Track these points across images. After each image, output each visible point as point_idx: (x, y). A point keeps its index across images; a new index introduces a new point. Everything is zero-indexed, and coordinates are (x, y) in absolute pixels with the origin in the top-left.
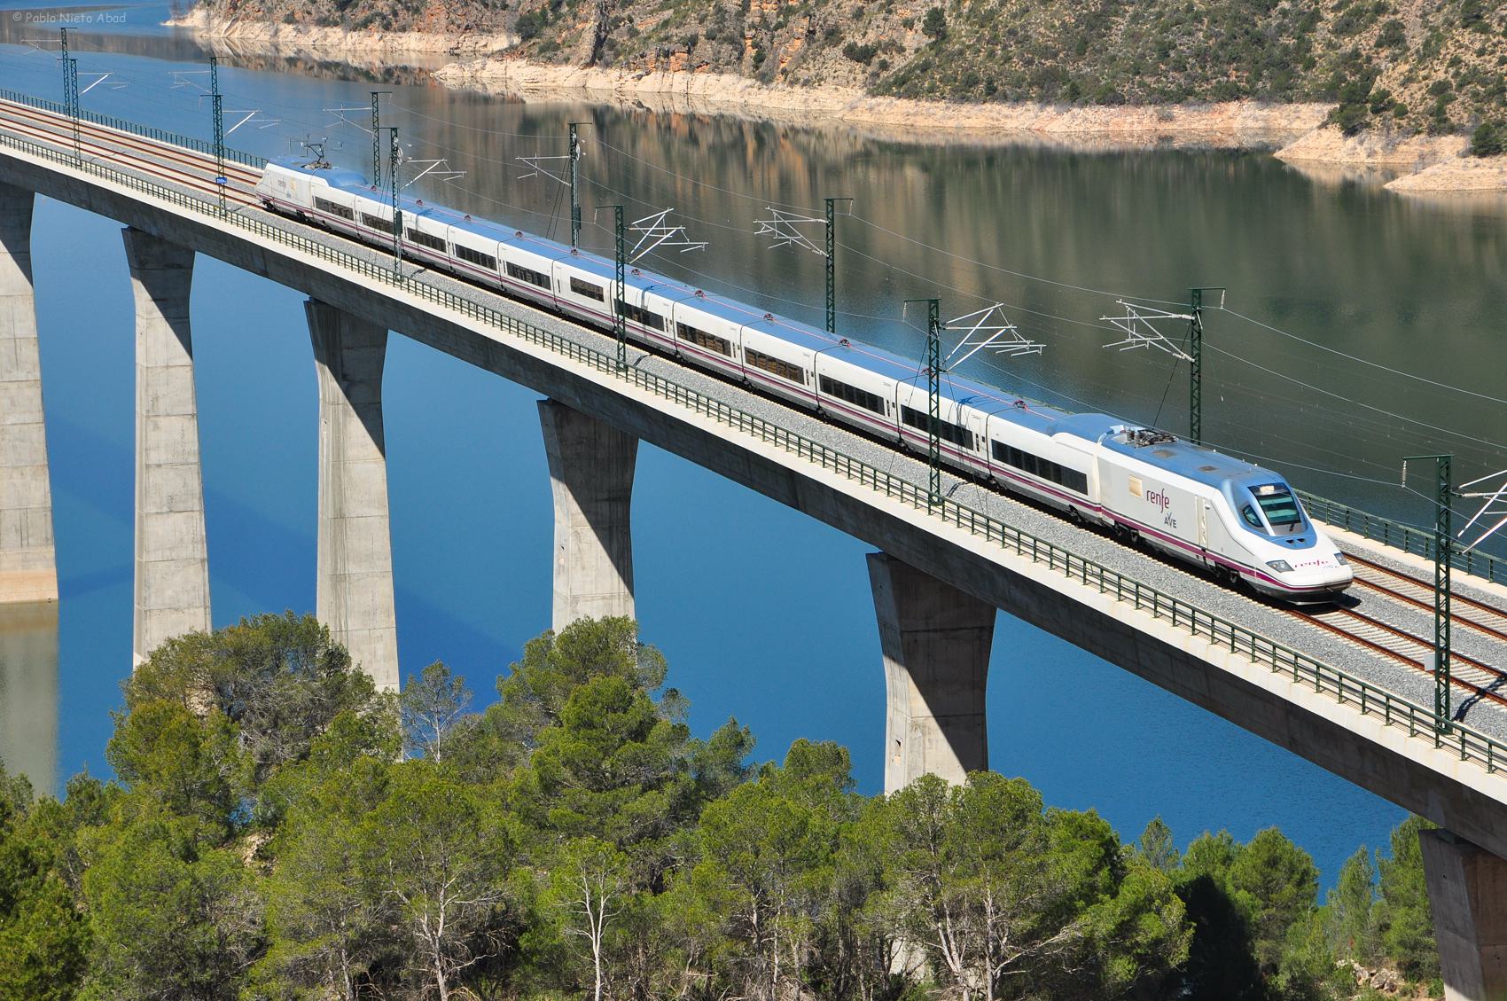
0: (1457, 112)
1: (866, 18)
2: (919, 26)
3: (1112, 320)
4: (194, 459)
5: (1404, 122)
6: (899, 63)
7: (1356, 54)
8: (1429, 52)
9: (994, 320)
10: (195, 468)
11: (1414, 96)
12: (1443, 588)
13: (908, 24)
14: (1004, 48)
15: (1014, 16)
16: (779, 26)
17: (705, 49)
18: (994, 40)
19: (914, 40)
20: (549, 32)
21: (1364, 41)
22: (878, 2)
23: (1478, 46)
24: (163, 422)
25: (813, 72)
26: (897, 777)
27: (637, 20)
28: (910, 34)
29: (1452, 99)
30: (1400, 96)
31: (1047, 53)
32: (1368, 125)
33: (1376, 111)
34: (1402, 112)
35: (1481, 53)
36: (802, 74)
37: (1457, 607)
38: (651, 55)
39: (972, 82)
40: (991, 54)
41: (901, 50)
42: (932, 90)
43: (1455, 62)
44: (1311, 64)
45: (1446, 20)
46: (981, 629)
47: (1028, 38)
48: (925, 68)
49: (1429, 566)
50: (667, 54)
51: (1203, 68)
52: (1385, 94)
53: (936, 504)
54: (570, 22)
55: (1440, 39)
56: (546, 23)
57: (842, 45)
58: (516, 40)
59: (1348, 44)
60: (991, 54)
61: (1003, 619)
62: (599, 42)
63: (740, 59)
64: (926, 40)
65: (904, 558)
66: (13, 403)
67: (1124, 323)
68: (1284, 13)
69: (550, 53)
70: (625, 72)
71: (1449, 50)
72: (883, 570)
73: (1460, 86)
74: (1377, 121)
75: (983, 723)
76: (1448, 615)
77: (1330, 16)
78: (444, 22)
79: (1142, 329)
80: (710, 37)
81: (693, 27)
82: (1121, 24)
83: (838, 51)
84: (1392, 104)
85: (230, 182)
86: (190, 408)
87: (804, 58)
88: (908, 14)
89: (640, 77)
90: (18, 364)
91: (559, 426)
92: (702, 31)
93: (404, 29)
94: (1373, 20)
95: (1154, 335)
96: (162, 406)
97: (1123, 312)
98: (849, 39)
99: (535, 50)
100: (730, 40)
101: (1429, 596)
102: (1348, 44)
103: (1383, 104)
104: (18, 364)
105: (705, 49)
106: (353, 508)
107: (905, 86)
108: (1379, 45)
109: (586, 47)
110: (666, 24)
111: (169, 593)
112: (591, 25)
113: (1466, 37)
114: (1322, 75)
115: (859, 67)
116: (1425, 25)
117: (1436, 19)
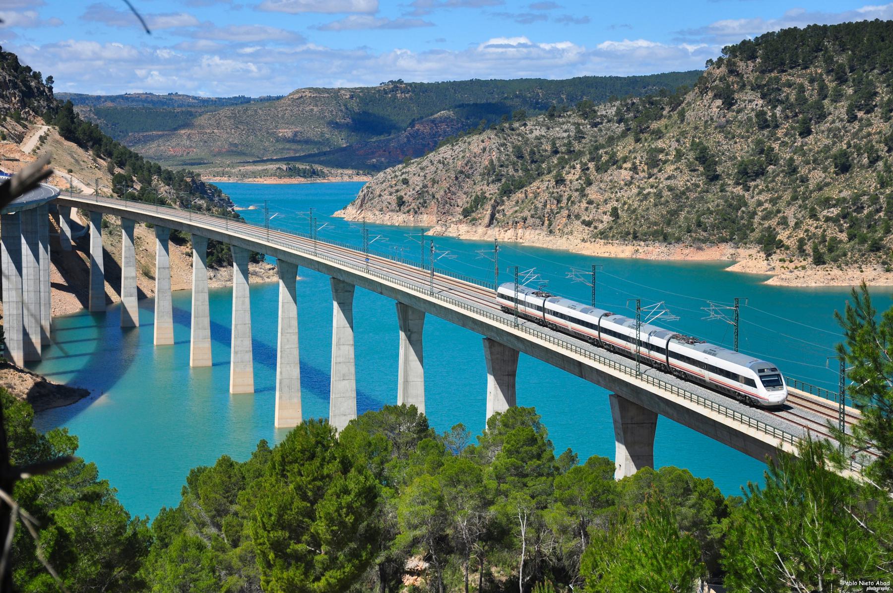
0: (808, 248)
1: (589, 211)
2: (609, 214)
3: (705, 309)
4: (352, 361)
5: (788, 252)
6: (601, 226)
7: (770, 227)
8: (797, 225)
9: (661, 308)
10: (353, 364)
11: (792, 243)
12: (843, 412)
13: (605, 213)
14: (640, 222)
15: (644, 211)
16: (557, 213)
17: (530, 221)
18: (637, 219)
19: (607, 218)
20: (474, 215)
21: (773, 222)
22: (224, 589)
23: (815, 225)
24: (342, 347)
25: (569, 229)
26: (619, 475)
27: (506, 211)
28: (605, 217)
29: (806, 244)
30: (787, 242)
31: (656, 224)
32: (775, 253)
33: (777, 248)
34: (788, 248)
35: (816, 228)
36: (566, 230)
37: (847, 419)
38: (510, 223)
39: (628, 233)
40: (635, 224)
41: (602, 222)
42: (613, 236)
43: (807, 231)
44: (753, 230)
45: (803, 216)
46: (652, 423)
47: (648, 219)
48: (611, 228)
49: (836, 405)
50: (516, 223)
51: (713, 231)
52: (781, 241)
53: (639, 375)
54: (482, 211)
55: (802, 222)
56: (473, 212)
57: (581, 220)
58: (461, 217)
59: (766, 224)
60: (635, 224)
61: (661, 419)
62: (492, 217)
63: (543, 225)
64: (611, 219)
65: (624, 396)
66: (288, 341)
67: (710, 310)
68: (743, 212)
69: (474, 222)
70: (501, 229)
71: (804, 227)
72: (615, 401)
73: (809, 240)
74: (778, 251)
75: (652, 459)
76: (844, 422)
77: (760, 213)
78: (436, 211)
79: (716, 312)
80: (532, 217)
81: (526, 213)
82: (683, 214)
83: (579, 222)
84: (783, 246)
85: (364, 259)
86: (352, 342)
87: (566, 224)
88: (605, 210)
89: (506, 231)
90: (290, 327)
91: (490, 348)
92: (529, 214)
93: (421, 213)
94: (776, 215)
95: (720, 314)
96: (342, 341)
97: (709, 305)
98: (583, 218)
99: (469, 221)
100: (540, 218)
101: (837, 415)
102: (766, 224)
103: (780, 245)
104: (290, 327)
105: (530, 221)
106: (411, 378)
107: (603, 235)
108: (778, 224)
109: (487, 220)
110: (516, 212)
111: (342, 409)
112: (489, 212)
113: (811, 222)
114: (756, 234)
115: (587, 228)
116: (795, 217)
117: (800, 216)
